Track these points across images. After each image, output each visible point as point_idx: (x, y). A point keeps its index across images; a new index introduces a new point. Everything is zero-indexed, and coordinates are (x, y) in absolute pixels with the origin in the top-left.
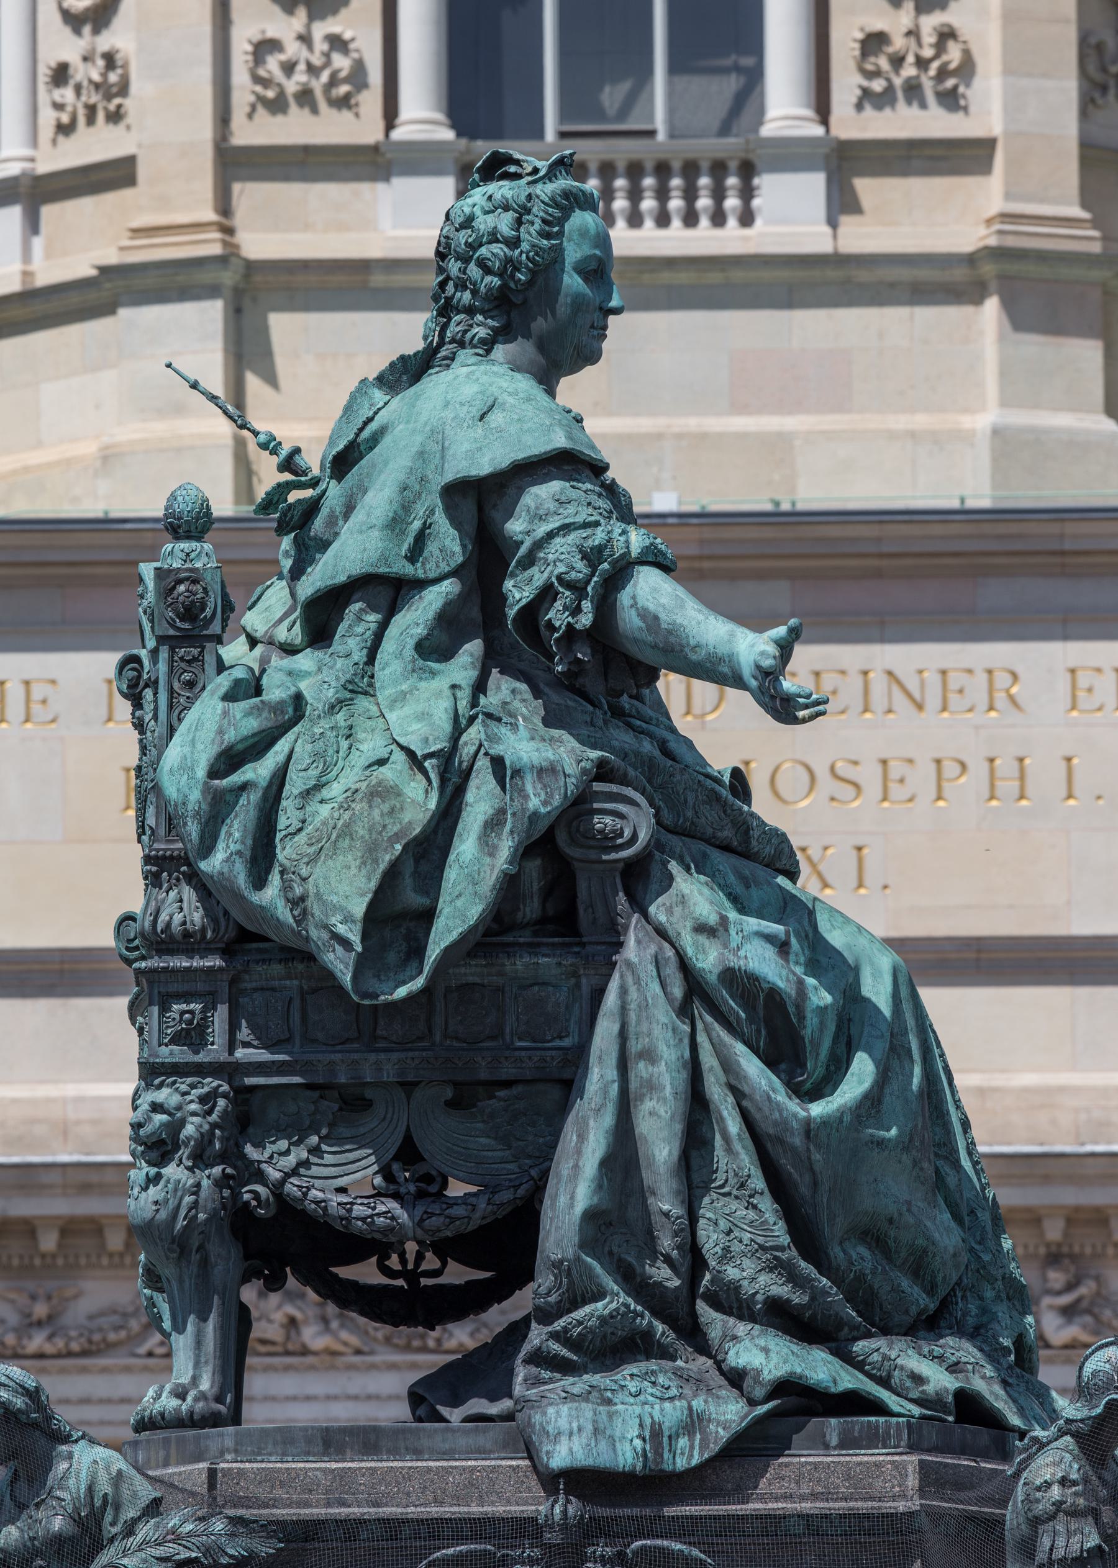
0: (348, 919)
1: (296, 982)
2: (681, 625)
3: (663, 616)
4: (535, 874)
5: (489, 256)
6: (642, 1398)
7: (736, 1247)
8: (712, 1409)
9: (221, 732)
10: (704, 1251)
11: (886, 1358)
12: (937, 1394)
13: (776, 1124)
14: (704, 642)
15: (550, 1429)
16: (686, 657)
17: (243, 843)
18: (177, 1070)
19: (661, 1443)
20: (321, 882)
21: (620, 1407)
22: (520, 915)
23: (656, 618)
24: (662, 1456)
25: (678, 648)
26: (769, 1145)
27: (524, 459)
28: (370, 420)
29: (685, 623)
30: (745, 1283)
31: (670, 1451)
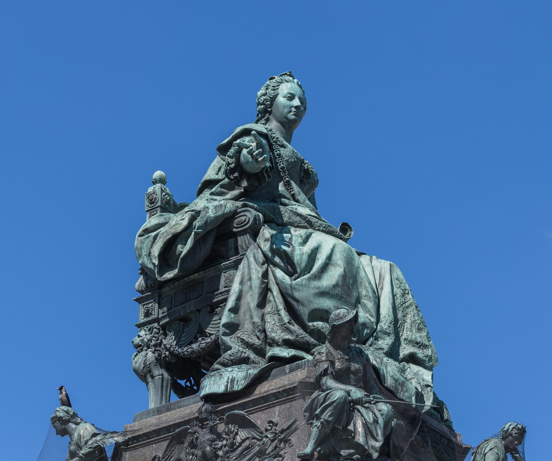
7: (275, 328)
17: (147, 252)
24: (234, 387)
31: (237, 384)
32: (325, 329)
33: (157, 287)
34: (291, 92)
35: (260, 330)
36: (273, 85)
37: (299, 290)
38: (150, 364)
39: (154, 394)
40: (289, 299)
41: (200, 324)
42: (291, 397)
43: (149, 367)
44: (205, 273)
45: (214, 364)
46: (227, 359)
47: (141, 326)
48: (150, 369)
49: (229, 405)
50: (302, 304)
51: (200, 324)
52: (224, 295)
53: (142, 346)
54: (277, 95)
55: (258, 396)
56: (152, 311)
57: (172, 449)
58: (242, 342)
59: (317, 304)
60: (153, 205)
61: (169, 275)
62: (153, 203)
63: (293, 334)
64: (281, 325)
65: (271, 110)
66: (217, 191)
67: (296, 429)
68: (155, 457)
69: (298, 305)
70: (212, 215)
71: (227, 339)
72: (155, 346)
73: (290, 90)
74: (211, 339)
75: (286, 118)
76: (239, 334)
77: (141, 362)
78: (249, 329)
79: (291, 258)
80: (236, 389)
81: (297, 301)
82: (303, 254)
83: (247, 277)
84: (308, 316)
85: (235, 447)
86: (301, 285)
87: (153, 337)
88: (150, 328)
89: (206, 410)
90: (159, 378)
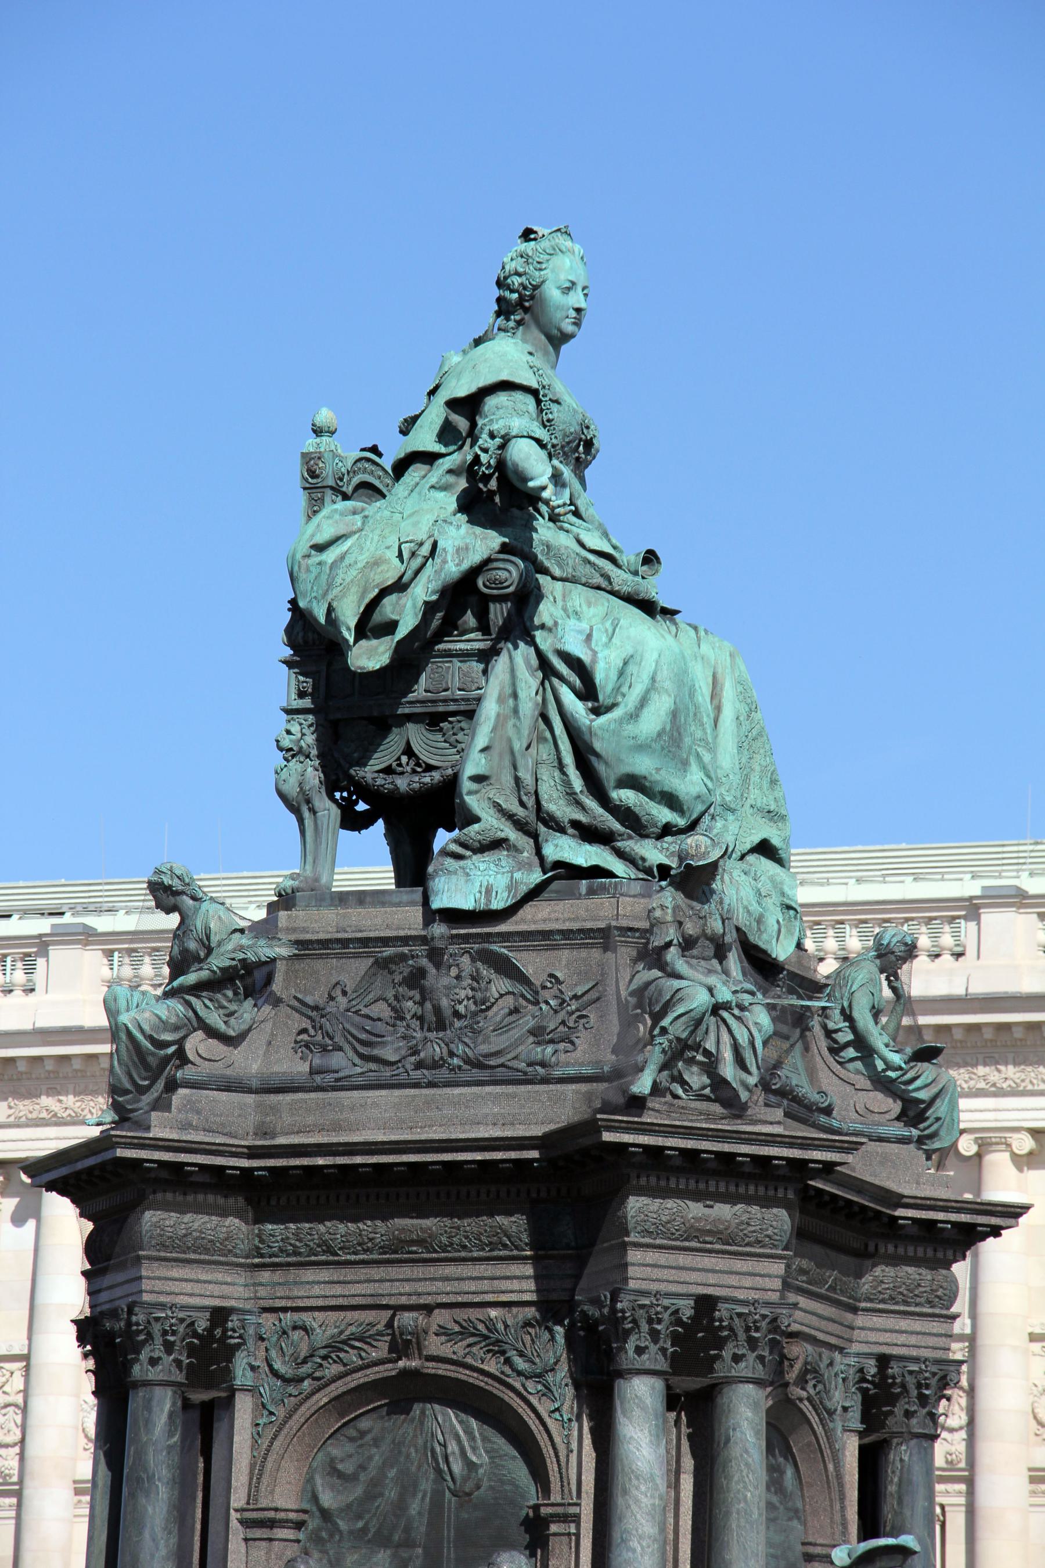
41: (408, 743)
62: (317, 477)
68: (337, 983)
70: (454, 569)
81: (597, 755)
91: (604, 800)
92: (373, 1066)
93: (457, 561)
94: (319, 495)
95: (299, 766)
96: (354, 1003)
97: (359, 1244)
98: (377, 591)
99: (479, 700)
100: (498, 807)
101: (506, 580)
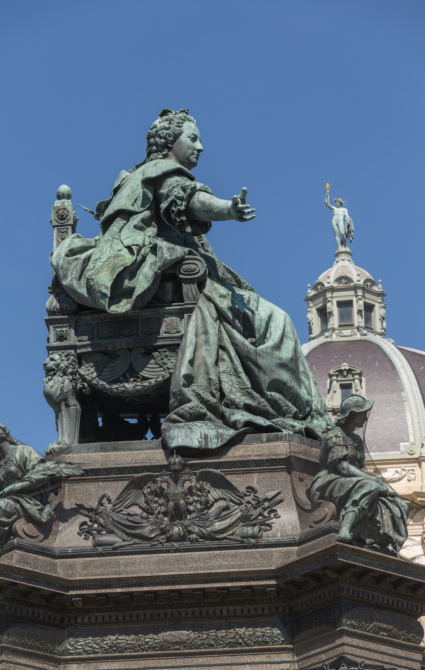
0: (106, 287)
1: (95, 321)
2: (212, 203)
3: (206, 201)
4: (170, 287)
5: (161, 133)
6: (202, 428)
7: (234, 390)
8: (225, 432)
9: (70, 245)
10: (224, 390)
11: (283, 422)
12: (299, 429)
13: (246, 352)
14: (218, 206)
15: (171, 436)
16: (214, 212)
17: (76, 275)
18: (57, 348)
19: (208, 440)
20: (98, 279)
21: (194, 430)
22: (165, 299)
23: (205, 202)
25: (211, 210)
26: (244, 360)
27: (166, 171)
28: (125, 178)
29: (213, 202)
30: (237, 399)
31: (211, 442)
32: (281, 401)
33: (72, 312)
34: (195, 133)
35: (217, 388)
36: (178, 121)
37: (263, 357)
38: (67, 392)
39: (68, 424)
40: (249, 363)
41: (131, 364)
42: (274, 467)
43: (66, 395)
44: (141, 312)
45: (171, 414)
46: (186, 412)
47: (50, 349)
48: (67, 398)
49: (200, 461)
50: (264, 372)
51: (131, 364)
52: (166, 341)
53: (55, 371)
54: (181, 134)
55: (231, 459)
56: (67, 336)
57: (129, 492)
58: (197, 396)
59: (278, 375)
60: (63, 222)
61: (116, 309)
62: (64, 219)
63: (255, 400)
64: (242, 389)
65: (172, 147)
66: (139, 225)
67: (281, 501)
68: (104, 496)
69: (259, 372)
70: (169, 258)
71: (185, 390)
72: (71, 374)
73: (194, 131)
74: (150, 384)
75: (188, 159)
76: (194, 387)
77: (58, 388)
78: (203, 384)
79: (252, 322)
80: (211, 447)
82: (262, 319)
83: (201, 330)
84: (268, 385)
85: (209, 505)
86: (266, 353)
87: (71, 364)
88: (68, 354)
89: (180, 463)
90: (75, 409)
91: (263, 395)
92: (137, 541)
93: (169, 254)
94: (65, 230)
95: (60, 379)
96: (117, 506)
97: (139, 646)
98: (122, 268)
99: (181, 337)
100: (198, 395)
101: (195, 270)
